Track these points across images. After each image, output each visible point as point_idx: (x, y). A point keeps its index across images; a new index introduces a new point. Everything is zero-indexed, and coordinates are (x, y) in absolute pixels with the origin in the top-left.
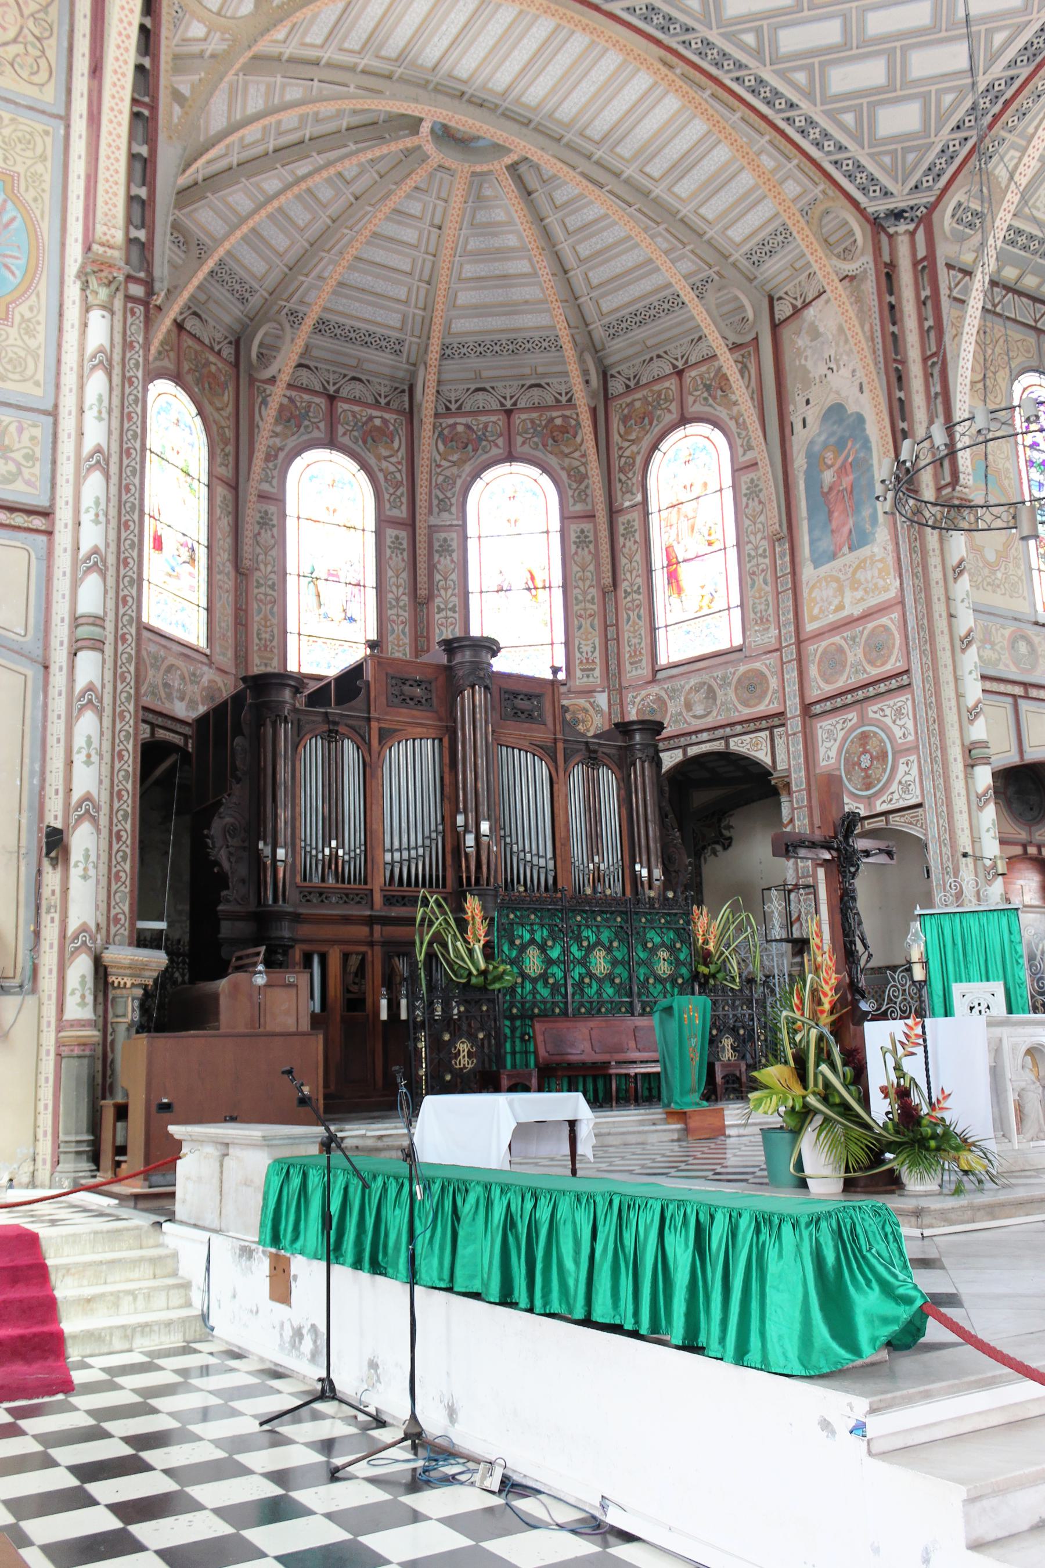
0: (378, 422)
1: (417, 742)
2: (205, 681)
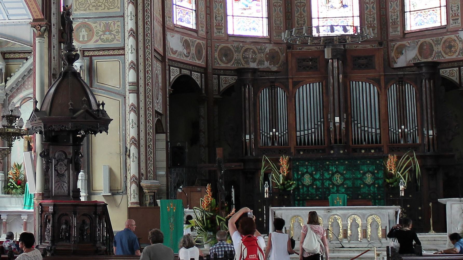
1: (311, 84)
2: (267, 50)
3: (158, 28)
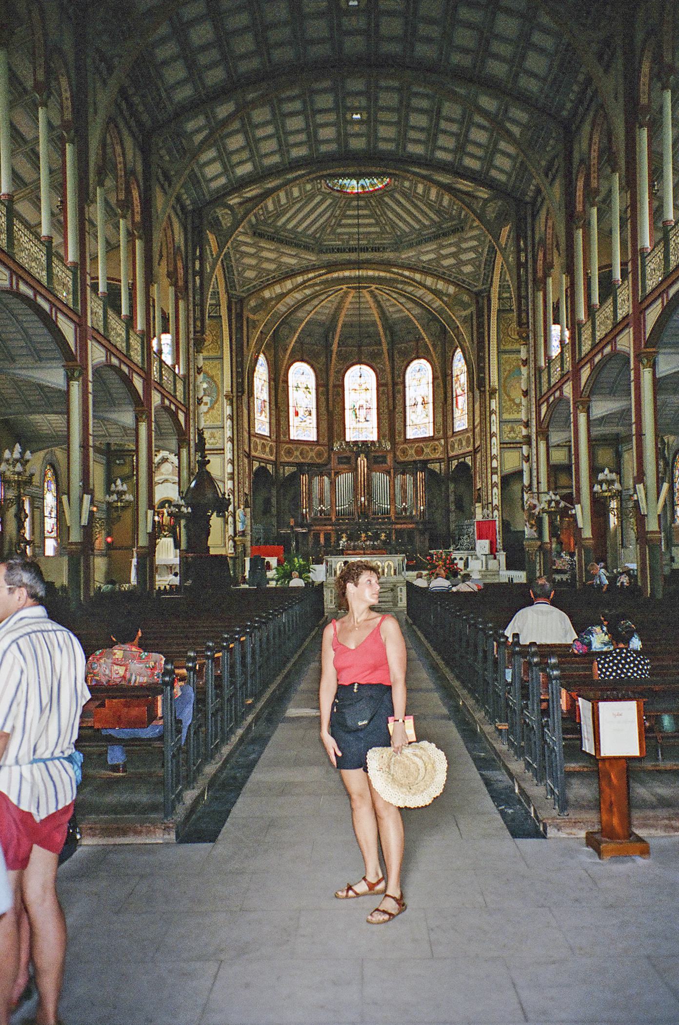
0: (376, 351)
3: (246, 435)
